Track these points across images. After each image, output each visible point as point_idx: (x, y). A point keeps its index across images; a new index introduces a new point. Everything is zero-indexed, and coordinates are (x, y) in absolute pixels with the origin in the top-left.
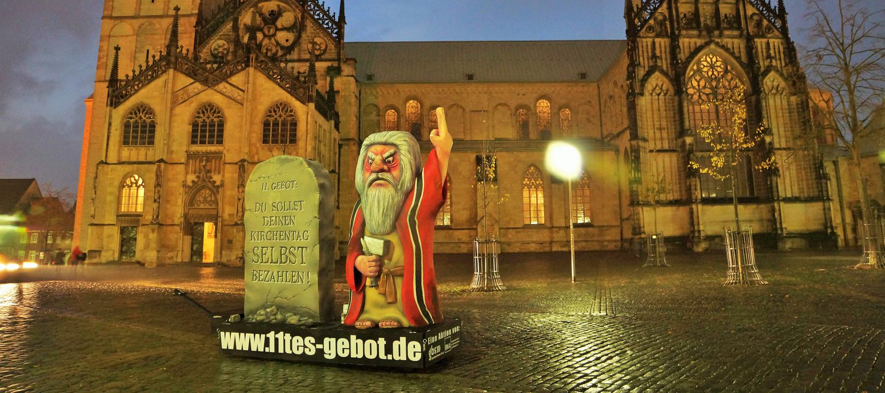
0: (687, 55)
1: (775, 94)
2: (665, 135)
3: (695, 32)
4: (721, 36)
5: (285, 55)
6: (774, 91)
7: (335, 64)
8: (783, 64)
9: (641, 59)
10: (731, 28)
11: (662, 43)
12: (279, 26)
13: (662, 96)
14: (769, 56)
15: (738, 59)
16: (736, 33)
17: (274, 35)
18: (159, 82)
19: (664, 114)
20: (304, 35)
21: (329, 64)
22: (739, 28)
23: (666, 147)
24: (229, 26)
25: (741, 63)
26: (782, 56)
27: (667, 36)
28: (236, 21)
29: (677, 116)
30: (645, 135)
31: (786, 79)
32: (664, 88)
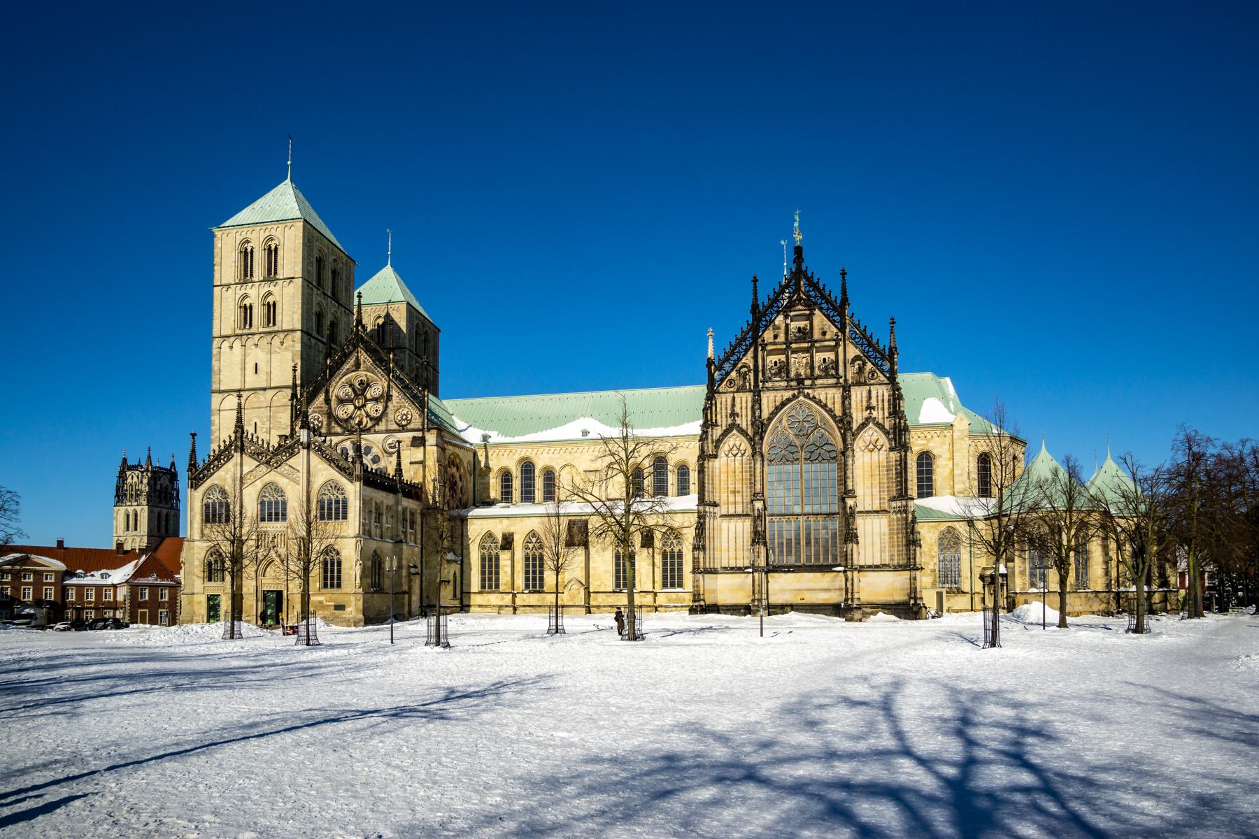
0: (772, 409)
1: (872, 451)
2: (739, 499)
3: (785, 384)
4: (812, 387)
6: (871, 447)
7: (419, 434)
8: (886, 414)
10: (827, 376)
11: (745, 399)
12: (368, 396)
13: (738, 458)
14: (869, 408)
15: (830, 412)
16: (833, 381)
17: (364, 406)
19: (739, 476)
20: (390, 404)
21: (411, 434)
22: (837, 376)
23: (739, 511)
24: (321, 397)
25: (834, 417)
26: (886, 404)
28: (327, 392)
31: (887, 433)
32: (742, 448)
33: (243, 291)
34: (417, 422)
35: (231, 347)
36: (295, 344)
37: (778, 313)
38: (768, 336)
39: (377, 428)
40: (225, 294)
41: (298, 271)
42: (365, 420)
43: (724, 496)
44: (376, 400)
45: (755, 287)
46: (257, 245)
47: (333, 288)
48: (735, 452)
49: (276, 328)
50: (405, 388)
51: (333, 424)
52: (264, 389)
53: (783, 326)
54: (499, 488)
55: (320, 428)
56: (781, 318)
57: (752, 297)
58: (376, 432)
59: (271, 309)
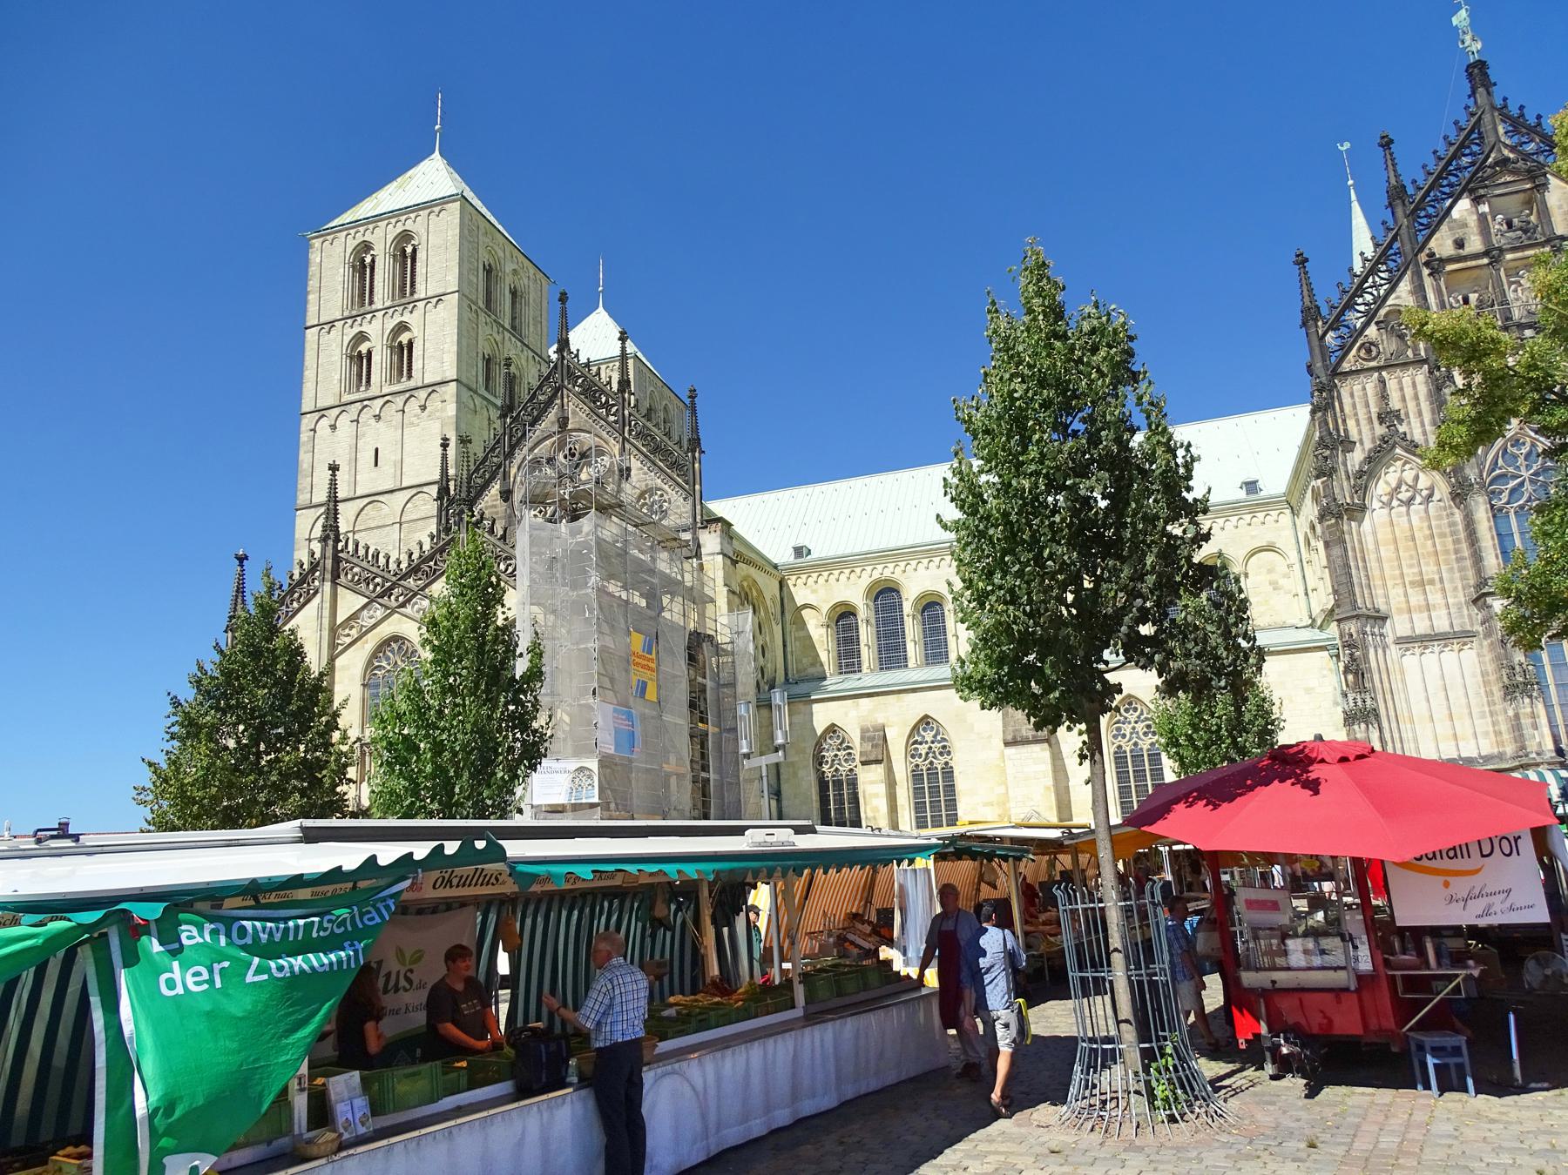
9: (1351, 423)
13: (1417, 507)
23: (1442, 625)
27: (1421, 362)
28: (506, 476)
29: (1464, 545)
30: (1381, 604)
33: (356, 329)
35: (333, 427)
36: (446, 406)
40: (325, 338)
41: (452, 281)
43: (1396, 595)
47: (514, 318)
48: (1404, 496)
49: (412, 384)
53: (1472, 220)
54: (832, 645)
59: (403, 353)
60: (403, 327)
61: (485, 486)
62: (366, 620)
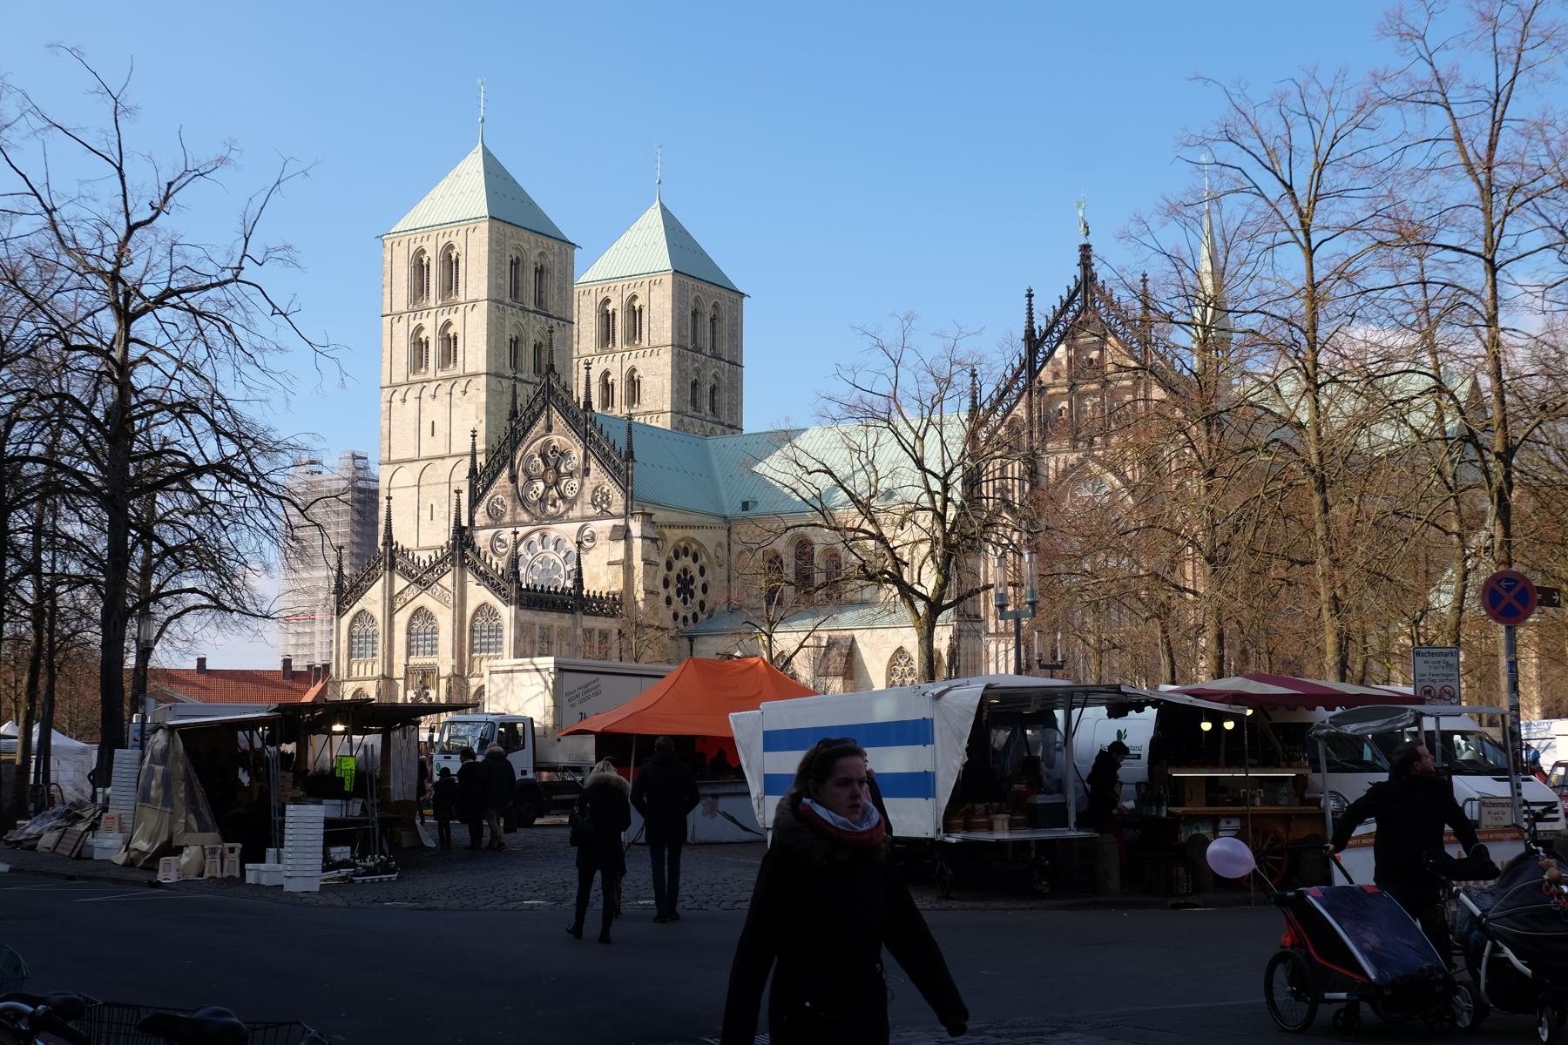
5: (567, 511)
7: (621, 522)
12: (563, 470)
17: (556, 483)
18: (381, 580)
21: (611, 523)
24: (506, 473)
28: (512, 466)
34: (618, 503)
35: (404, 401)
36: (479, 391)
37: (1059, 342)
38: (1045, 375)
39: (571, 514)
42: (559, 502)
44: (571, 474)
45: (1030, 305)
46: (432, 255)
49: (459, 371)
50: (605, 460)
51: (519, 510)
52: (443, 458)
55: (503, 514)
56: (1062, 348)
57: (1025, 318)
58: (570, 521)
59: (449, 343)
60: (448, 324)
61: (500, 470)
62: (409, 595)
